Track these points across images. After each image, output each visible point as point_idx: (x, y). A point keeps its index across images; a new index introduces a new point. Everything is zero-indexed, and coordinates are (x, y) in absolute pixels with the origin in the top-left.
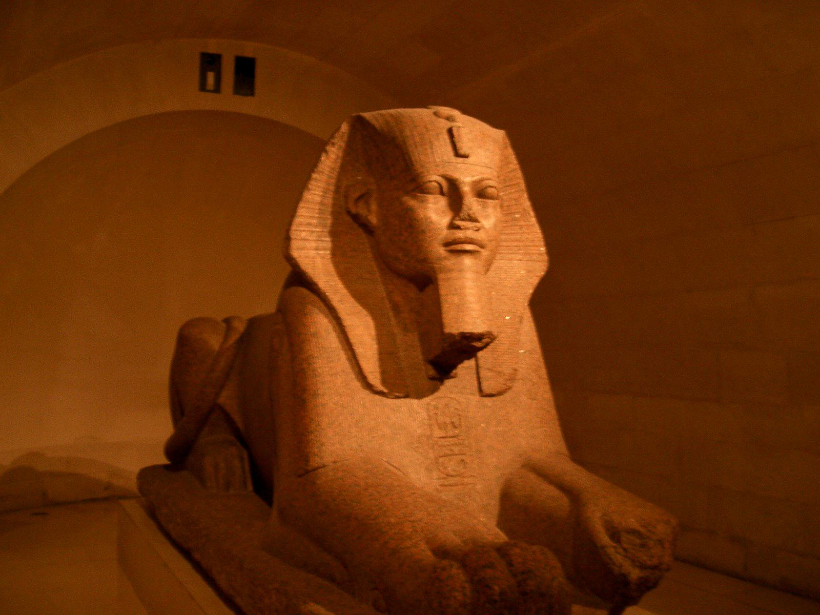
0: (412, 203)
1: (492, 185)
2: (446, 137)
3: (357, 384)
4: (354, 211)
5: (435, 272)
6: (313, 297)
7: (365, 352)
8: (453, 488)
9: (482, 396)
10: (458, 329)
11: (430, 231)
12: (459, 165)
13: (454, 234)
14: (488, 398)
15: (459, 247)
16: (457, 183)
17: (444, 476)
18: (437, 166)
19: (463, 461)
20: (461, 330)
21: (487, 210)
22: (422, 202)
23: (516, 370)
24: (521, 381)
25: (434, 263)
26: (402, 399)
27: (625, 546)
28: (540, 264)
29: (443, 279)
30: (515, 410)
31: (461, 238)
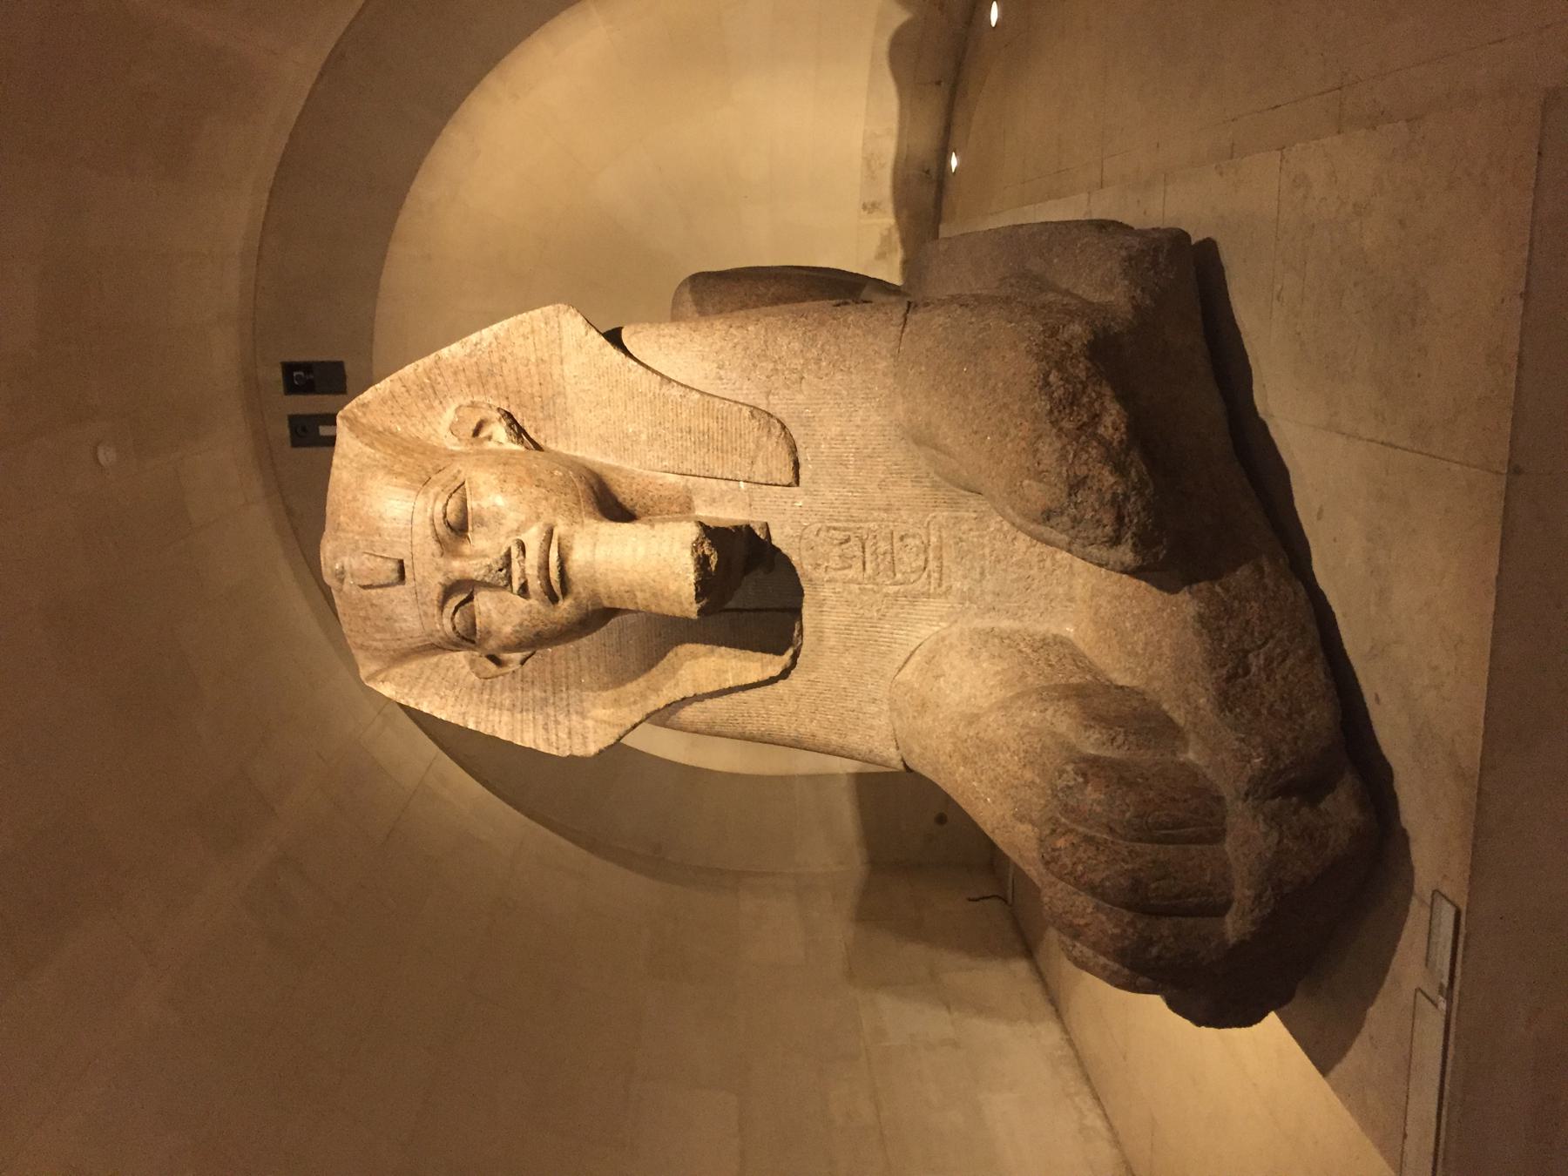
1: (442, 515)
2: (373, 592)
3: (781, 686)
7: (732, 668)
8: (945, 563)
9: (797, 483)
10: (691, 603)
11: (534, 626)
12: (419, 578)
13: (535, 592)
14: (801, 471)
15: (556, 586)
16: (449, 584)
17: (925, 575)
19: (902, 538)
21: (486, 519)
24: (771, 397)
25: (587, 610)
28: (563, 323)
29: (611, 603)
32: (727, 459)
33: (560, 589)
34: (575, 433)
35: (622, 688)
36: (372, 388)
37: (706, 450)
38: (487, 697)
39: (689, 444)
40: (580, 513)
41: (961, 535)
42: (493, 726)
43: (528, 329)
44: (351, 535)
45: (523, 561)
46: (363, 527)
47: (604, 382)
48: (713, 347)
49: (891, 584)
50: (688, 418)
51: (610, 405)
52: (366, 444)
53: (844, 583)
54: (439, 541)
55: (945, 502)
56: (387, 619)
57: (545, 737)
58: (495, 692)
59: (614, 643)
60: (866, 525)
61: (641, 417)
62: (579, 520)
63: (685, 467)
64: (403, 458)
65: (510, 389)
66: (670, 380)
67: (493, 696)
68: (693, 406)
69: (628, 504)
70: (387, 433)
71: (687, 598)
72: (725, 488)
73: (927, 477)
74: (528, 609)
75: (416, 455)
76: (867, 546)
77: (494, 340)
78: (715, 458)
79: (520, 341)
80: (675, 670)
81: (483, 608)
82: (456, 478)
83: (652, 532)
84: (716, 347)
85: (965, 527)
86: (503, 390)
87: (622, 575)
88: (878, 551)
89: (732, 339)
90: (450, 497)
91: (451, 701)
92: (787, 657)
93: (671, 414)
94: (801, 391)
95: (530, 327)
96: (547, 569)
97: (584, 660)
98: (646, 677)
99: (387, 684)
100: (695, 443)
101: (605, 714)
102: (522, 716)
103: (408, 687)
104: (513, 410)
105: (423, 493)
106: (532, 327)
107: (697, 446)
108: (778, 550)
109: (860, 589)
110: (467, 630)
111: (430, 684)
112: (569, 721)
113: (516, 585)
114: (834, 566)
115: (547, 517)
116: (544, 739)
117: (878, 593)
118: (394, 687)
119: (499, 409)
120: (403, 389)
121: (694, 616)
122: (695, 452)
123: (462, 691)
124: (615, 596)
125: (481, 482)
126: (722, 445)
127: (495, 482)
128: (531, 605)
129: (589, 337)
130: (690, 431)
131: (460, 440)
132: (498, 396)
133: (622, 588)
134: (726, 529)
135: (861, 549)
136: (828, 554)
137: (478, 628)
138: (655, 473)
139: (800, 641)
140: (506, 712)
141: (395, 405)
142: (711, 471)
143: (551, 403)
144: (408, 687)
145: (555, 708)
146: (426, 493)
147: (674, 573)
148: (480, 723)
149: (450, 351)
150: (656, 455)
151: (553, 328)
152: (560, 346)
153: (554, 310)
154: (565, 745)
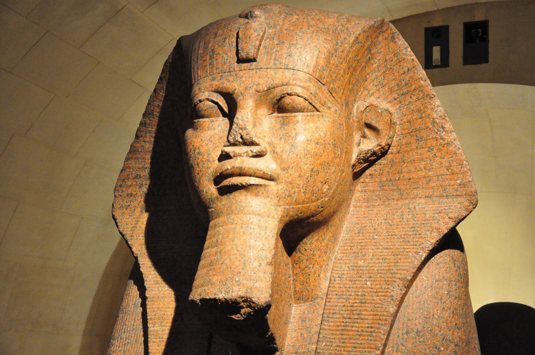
1: (289, 92)
2: (234, 40)
11: (198, 164)
12: (241, 73)
15: (226, 182)
16: (235, 96)
21: (285, 127)
28: (460, 199)
31: (228, 169)
32: (336, 335)
34: (369, 207)
36: (407, 44)
37: (345, 316)
39: (351, 301)
40: (288, 204)
43: (455, 170)
44: (281, 23)
45: (248, 156)
46: (285, 32)
47: (410, 231)
48: (436, 328)
50: (373, 301)
51: (389, 235)
52: (357, 38)
56: (213, 51)
61: (377, 261)
62: (282, 203)
63: (333, 298)
64: (344, 65)
65: (406, 155)
66: (408, 287)
68: (384, 306)
69: (301, 247)
70: (369, 56)
71: (205, 290)
72: (313, 331)
74: (211, 159)
75: (347, 76)
77: (446, 142)
78: (339, 324)
79: (445, 163)
81: (217, 124)
82: (323, 105)
83: (264, 264)
84: (436, 330)
86: (406, 149)
87: (231, 236)
89: (443, 346)
90: (305, 99)
93: (378, 286)
95: (458, 171)
96: (240, 175)
100: (352, 306)
104: (389, 156)
105: (310, 78)
106: (457, 173)
107: (349, 308)
113: (230, 150)
115: (283, 175)
119: (389, 146)
120: (406, 69)
121: (191, 297)
122: (344, 306)
124: (217, 229)
125: (318, 124)
126: (348, 331)
127: (317, 136)
128: (214, 161)
129: (447, 220)
130: (361, 303)
131: (362, 112)
132: (400, 145)
133: (220, 237)
134: (267, 328)
137: (200, 120)
138: (330, 271)
141: (393, 64)
142: (327, 319)
143: (395, 188)
146: (310, 80)
147: (227, 280)
148: (145, 126)
149: (437, 107)
150: (346, 272)
151: (457, 190)
152: (441, 196)
153: (472, 192)
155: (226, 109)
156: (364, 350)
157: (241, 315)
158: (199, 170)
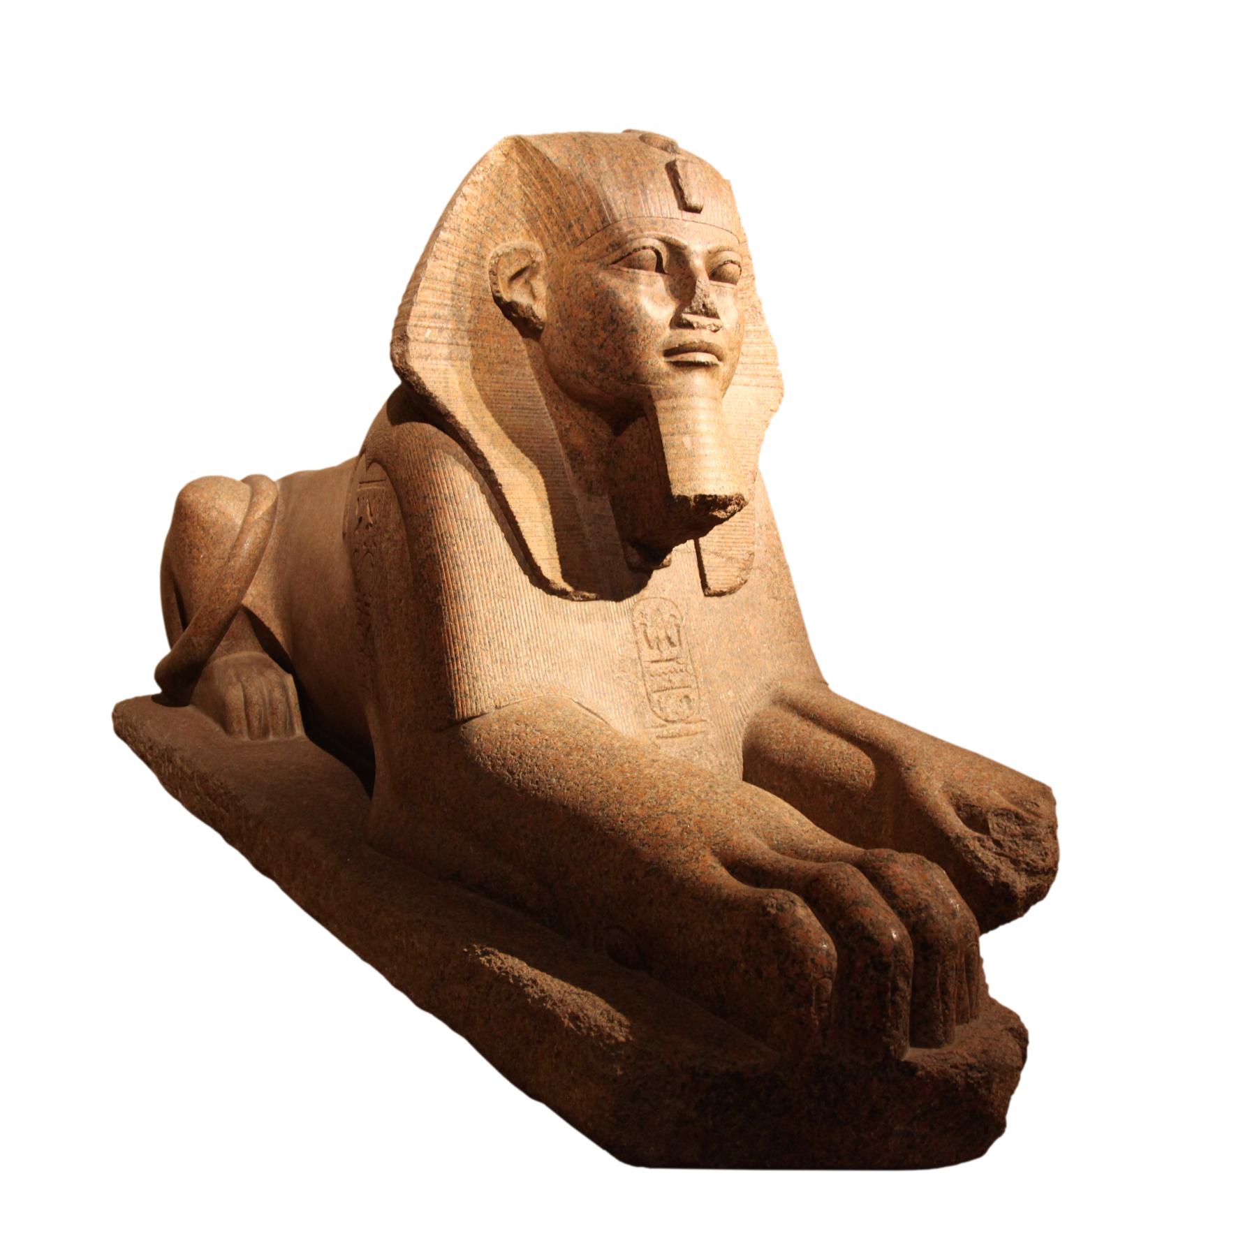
0: (613, 282)
2: (665, 176)
4: (506, 297)
5: (650, 397)
6: (443, 437)
8: (676, 740)
10: (695, 490)
11: (644, 329)
12: (687, 224)
13: (681, 335)
14: (715, 598)
16: (686, 252)
17: (663, 722)
18: (655, 223)
19: (687, 697)
20: (700, 492)
22: (632, 281)
23: (752, 554)
25: (650, 383)
26: (594, 602)
27: (995, 835)
29: (666, 410)
30: (755, 616)
31: (695, 342)
33: (685, 360)
35: (484, 406)
38: (470, 259)
41: (704, 752)
42: (442, 259)
49: (646, 689)
53: (637, 643)
54: (719, 251)
55: (726, 734)
57: (427, 314)
58: (473, 267)
59: (522, 402)
60: (689, 662)
67: (469, 265)
73: (743, 715)
74: (661, 325)
76: (671, 662)
80: (517, 464)
85: (712, 757)
88: (670, 674)
91: (471, 219)
92: (561, 584)
94: (769, 599)
95: (772, 361)
96: (706, 351)
97: (499, 369)
98: (502, 432)
99: (504, 159)
101: (454, 383)
102: (449, 293)
103: (496, 178)
108: (649, 576)
109: (635, 660)
110: (639, 260)
111: (493, 202)
112: (443, 343)
113: (688, 317)
114: (648, 631)
116: (425, 312)
117: (637, 677)
118: (499, 164)
123: (480, 234)
128: (665, 328)
133: (689, 422)
135: (669, 658)
136: (657, 626)
137: (636, 270)
139: (578, 598)
140: (454, 276)
144: (496, 178)
145: (455, 330)
148: (447, 246)
154: (419, 335)
155: (664, 263)
156: (743, 545)
157: (726, 512)
158: (646, 336)
